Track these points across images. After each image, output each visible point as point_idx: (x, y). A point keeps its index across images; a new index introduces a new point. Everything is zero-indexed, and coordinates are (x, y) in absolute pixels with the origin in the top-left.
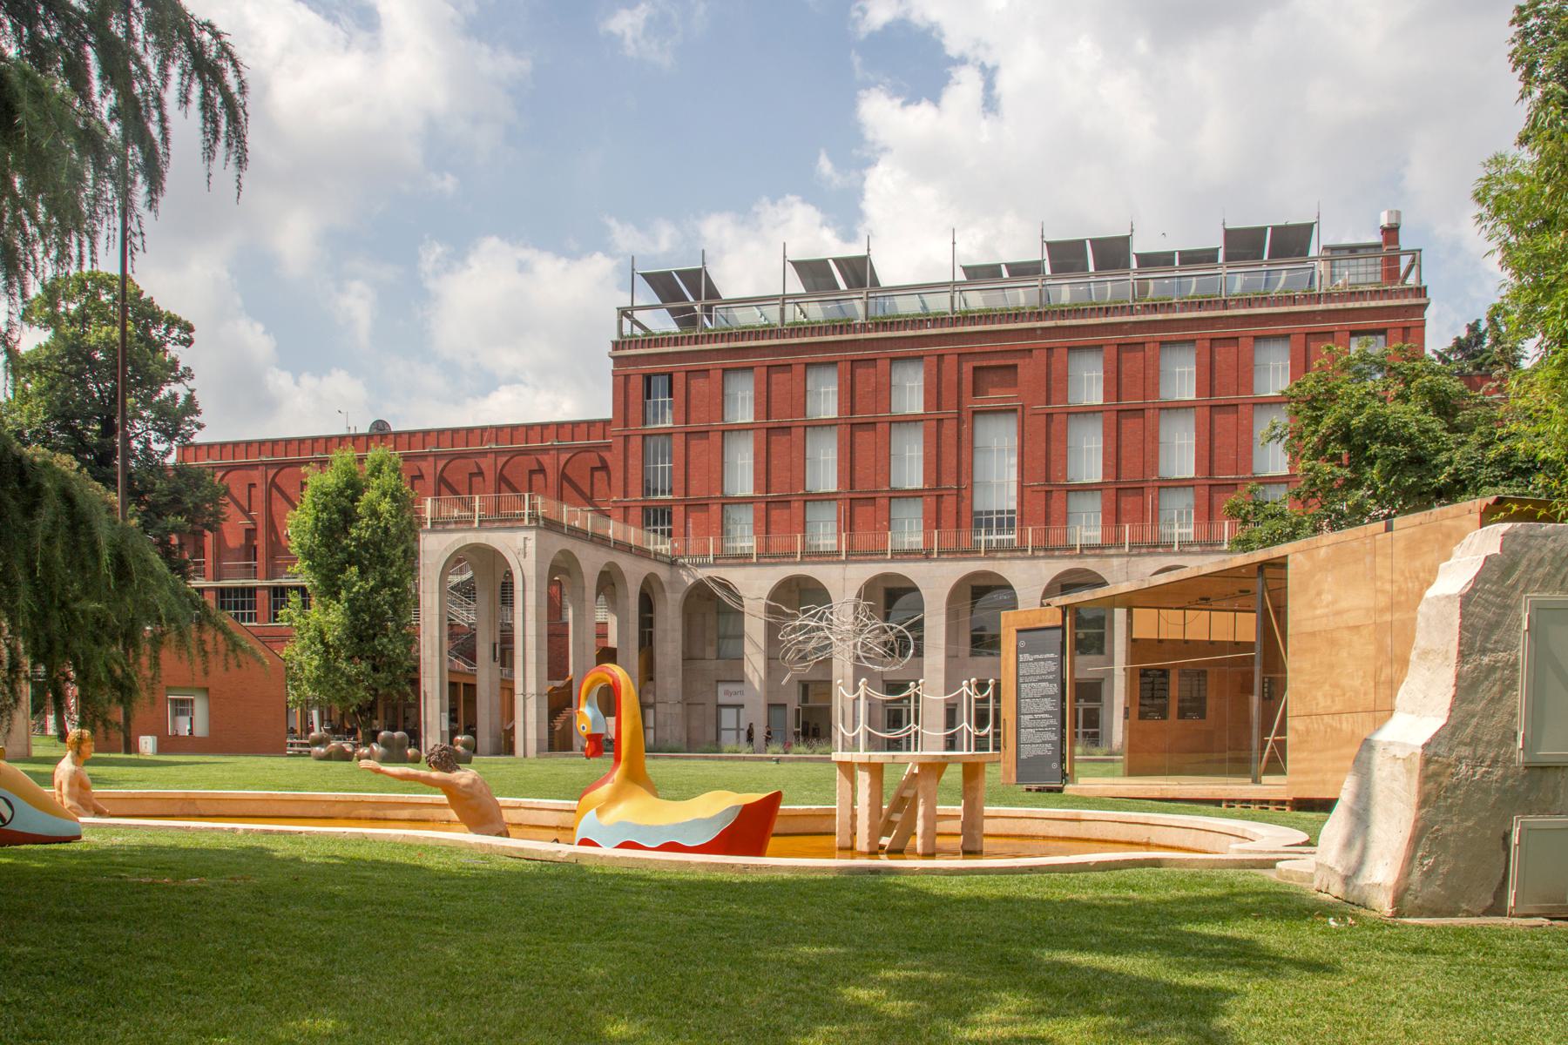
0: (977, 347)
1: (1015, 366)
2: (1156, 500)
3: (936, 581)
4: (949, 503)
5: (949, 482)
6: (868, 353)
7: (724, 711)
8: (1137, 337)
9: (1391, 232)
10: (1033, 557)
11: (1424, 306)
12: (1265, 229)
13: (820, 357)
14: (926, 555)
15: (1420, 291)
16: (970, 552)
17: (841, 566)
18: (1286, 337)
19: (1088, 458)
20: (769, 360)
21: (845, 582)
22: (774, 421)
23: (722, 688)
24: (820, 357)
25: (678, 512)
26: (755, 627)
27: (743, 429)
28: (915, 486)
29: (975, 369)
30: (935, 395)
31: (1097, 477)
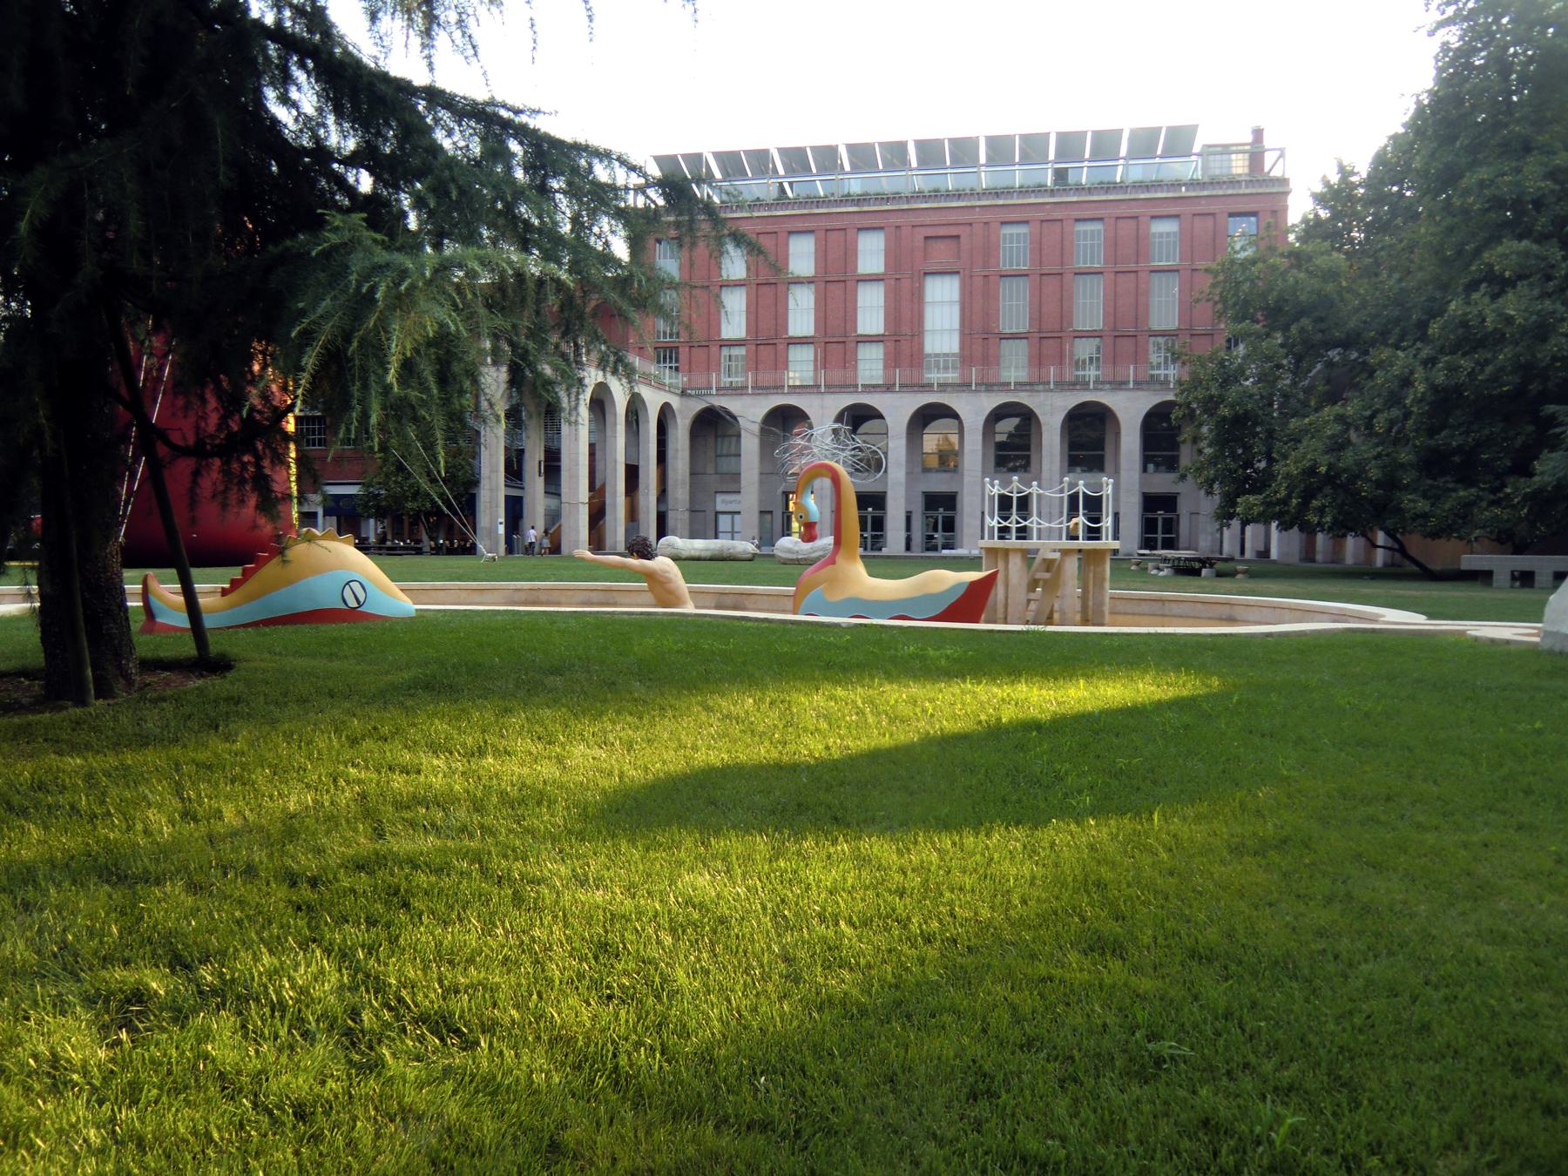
0: (928, 220)
1: (958, 237)
2: (1072, 346)
4: (905, 346)
5: (906, 330)
7: (721, 517)
8: (1057, 215)
11: (1287, 193)
12: (1160, 129)
13: (800, 225)
14: (888, 388)
16: (926, 387)
18: (1177, 216)
22: (761, 279)
23: (719, 498)
25: (684, 352)
26: (750, 444)
27: (738, 284)
28: (874, 332)
29: (926, 238)
30: (893, 256)
31: (1023, 328)
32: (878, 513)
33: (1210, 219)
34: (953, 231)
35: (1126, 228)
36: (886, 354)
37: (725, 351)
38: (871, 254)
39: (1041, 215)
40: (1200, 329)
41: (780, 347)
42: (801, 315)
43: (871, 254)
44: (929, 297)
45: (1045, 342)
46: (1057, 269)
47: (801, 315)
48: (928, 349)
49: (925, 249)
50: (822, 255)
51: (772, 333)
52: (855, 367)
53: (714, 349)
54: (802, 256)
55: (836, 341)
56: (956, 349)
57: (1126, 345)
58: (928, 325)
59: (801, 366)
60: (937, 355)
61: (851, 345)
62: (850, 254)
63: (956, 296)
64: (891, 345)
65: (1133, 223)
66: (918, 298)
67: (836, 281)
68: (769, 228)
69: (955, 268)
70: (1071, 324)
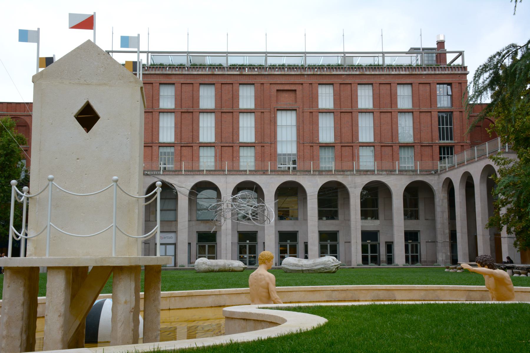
1: (295, 90)
2: (358, 151)
3: (270, 185)
5: (267, 140)
6: (229, 81)
9: (441, 44)
10: (313, 175)
13: (207, 80)
15: (465, 68)
17: (225, 176)
19: (326, 131)
20: (182, 81)
21: (226, 184)
24: (207, 80)
28: (249, 141)
29: (278, 90)
32: (253, 243)
33: (428, 86)
34: (293, 87)
35: (385, 89)
36: (256, 153)
37: (162, 150)
38: (247, 98)
39: (340, 81)
40: (425, 143)
41: (195, 148)
42: (207, 129)
43: (247, 98)
44: (279, 123)
45: (344, 148)
46: (349, 110)
47: (207, 129)
48: (279, 151)
49: (277, 97)
50: (219, 98)
51: (190, 140)
52: (239, 160)
53: (155, 148)
54: (207, 98)
55: (227, 145)
56: (294, 151)
57: (388, 150)
58: (279, 138)
59: (207, 159)
60: (285, 155)
61: (236, 148)
62: (235, 98)
63: (294, 123)
64: (259, 148)
65: (388, 87)
66: (273, 122)
67: (227, 113)
68: (188, 81)
69: (294, 108)
70: (358, 139)
